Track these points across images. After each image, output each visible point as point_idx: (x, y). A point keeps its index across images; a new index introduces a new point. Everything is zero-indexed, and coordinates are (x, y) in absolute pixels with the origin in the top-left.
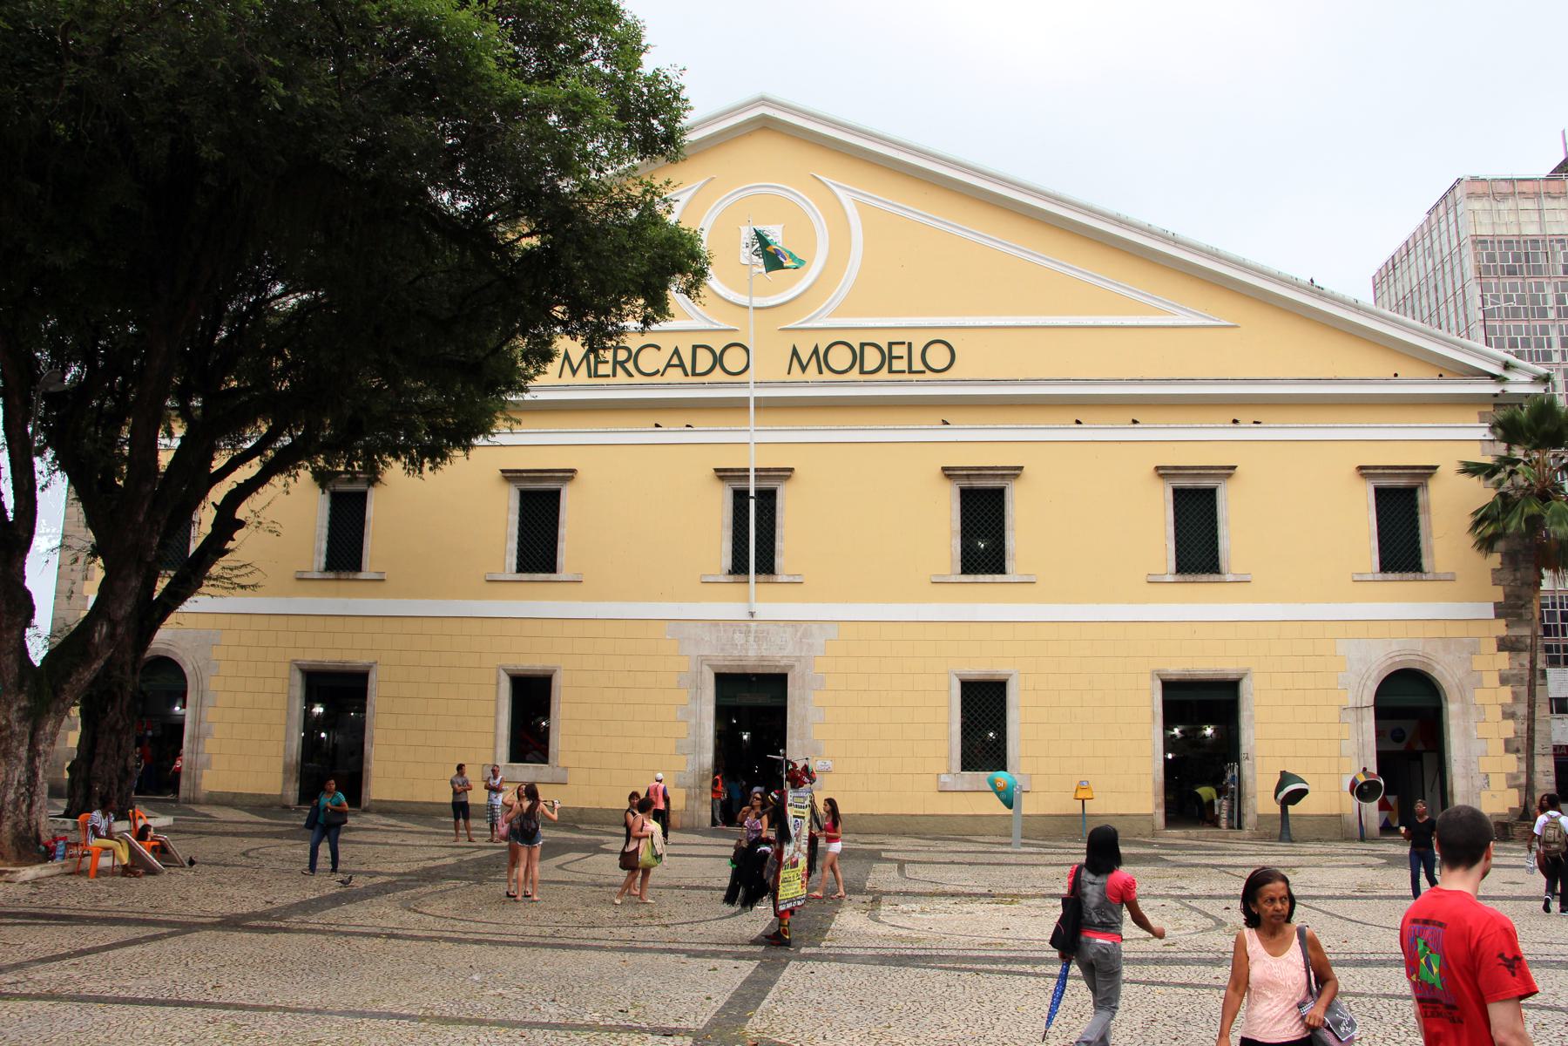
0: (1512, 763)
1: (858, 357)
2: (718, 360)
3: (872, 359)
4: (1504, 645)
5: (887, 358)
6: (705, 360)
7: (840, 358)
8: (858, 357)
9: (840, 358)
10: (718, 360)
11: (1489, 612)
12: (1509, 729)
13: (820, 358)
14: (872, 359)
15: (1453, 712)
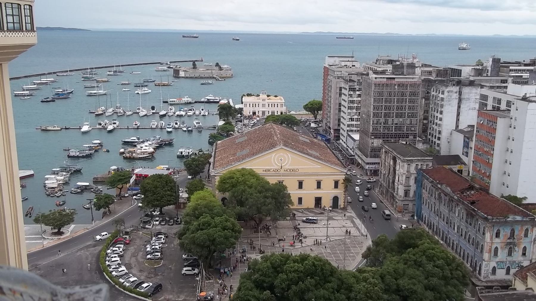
0: (343, 204)
1: (290, 170)
2: (277, 171)
3: (291, 171)
4: (344, 194)
5: (293, 170)
6: (276, 171)
7: (288, 170)
8: (290, 170)
9: (288, 170)
10: (277, 171)
11: (343, 191)
12: (343, 201)
13: (287, 170)
14: (291, 171)
15: (339, 199)
